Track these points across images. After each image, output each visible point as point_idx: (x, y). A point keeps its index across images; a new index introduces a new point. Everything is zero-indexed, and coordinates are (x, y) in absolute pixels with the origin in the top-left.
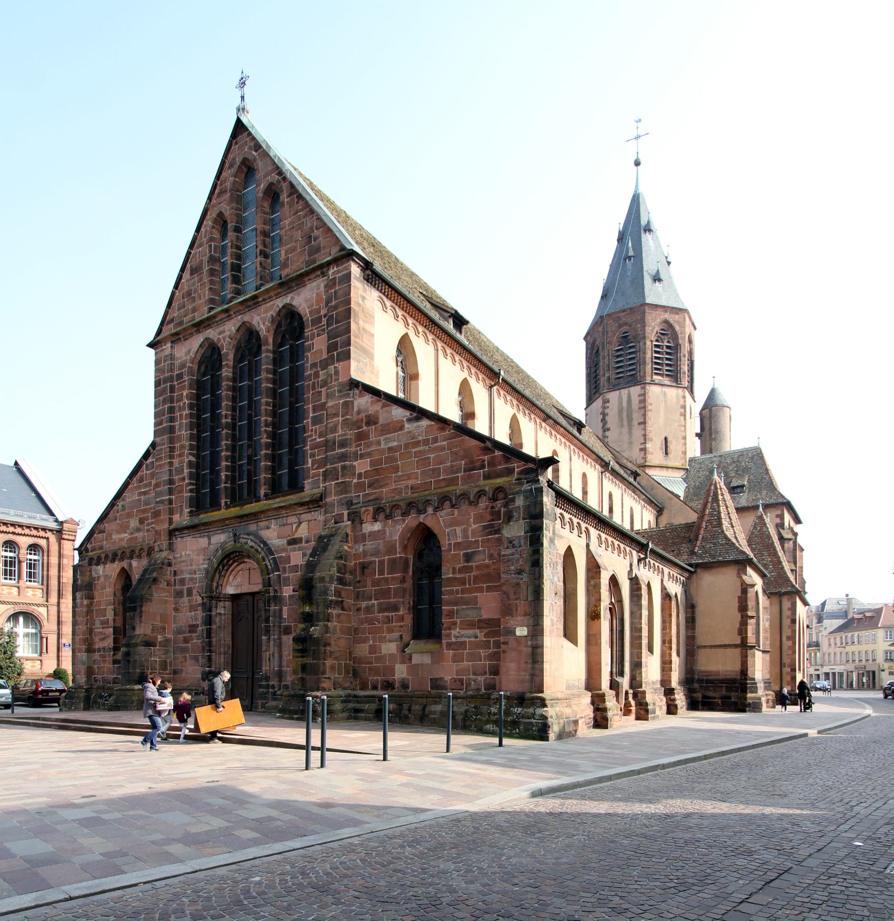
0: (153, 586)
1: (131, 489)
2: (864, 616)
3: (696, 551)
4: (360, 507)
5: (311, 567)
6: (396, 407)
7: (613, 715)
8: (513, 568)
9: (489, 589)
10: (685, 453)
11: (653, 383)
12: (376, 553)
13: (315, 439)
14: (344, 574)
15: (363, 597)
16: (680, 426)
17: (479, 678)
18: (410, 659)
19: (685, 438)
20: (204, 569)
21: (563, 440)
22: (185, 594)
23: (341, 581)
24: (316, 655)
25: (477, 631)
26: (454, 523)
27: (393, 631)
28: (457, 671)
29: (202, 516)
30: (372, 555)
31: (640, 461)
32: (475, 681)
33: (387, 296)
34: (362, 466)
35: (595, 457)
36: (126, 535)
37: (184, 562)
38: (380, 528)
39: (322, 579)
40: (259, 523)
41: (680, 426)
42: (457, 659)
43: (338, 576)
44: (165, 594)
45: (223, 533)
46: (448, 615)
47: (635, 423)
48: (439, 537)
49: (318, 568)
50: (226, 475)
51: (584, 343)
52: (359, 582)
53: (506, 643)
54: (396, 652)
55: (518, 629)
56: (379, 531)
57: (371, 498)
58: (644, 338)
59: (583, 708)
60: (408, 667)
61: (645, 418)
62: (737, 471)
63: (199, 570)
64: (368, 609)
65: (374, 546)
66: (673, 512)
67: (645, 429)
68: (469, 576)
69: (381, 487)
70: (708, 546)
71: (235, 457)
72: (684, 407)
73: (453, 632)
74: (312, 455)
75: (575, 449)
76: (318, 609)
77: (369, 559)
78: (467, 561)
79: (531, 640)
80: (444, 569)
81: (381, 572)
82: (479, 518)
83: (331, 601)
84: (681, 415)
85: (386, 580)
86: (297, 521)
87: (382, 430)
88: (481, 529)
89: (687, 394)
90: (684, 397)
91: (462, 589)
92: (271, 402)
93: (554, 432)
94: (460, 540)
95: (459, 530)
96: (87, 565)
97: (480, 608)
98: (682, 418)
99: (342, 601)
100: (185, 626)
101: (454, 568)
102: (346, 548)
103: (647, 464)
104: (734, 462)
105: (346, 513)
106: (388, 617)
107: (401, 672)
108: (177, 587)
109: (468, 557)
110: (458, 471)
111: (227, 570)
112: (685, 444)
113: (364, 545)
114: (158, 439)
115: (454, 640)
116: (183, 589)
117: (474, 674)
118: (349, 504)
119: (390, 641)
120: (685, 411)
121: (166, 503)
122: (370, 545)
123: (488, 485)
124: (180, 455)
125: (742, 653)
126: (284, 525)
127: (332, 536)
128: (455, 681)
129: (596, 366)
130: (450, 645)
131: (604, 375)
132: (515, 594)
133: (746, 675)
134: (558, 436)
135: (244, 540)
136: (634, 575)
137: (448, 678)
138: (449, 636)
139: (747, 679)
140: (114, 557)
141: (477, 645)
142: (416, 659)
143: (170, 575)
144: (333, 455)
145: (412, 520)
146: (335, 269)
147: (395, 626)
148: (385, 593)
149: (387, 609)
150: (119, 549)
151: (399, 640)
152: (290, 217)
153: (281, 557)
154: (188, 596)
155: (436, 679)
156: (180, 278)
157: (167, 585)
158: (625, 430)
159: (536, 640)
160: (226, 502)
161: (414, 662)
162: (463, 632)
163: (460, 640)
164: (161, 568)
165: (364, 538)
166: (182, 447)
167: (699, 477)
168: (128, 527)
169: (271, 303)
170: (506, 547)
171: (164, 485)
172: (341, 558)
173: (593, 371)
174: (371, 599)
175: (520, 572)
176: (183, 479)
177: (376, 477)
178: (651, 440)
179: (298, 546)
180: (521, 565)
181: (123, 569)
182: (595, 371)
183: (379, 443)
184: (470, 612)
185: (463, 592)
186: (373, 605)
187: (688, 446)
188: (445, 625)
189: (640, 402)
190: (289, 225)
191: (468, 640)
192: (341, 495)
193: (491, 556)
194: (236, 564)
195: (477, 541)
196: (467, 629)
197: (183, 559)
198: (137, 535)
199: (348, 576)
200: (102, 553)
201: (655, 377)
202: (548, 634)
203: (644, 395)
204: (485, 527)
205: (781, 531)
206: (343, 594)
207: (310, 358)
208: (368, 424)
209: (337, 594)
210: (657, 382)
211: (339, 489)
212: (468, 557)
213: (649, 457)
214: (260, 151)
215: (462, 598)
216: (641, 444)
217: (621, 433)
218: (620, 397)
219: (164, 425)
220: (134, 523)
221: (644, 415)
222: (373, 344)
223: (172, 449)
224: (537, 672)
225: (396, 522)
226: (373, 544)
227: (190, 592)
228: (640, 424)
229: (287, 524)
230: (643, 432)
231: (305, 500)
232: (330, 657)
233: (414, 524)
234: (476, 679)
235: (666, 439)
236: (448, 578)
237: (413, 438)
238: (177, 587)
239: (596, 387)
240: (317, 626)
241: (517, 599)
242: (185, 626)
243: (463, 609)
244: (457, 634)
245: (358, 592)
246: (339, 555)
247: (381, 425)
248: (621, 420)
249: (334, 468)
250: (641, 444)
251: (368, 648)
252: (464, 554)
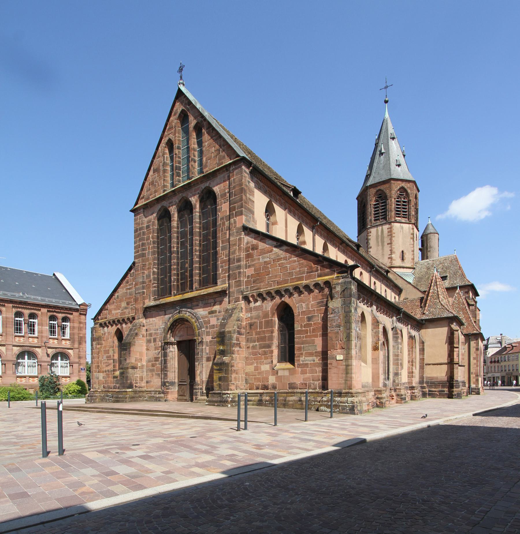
0: (136, 338)
1: (122, 287)
2: (512, 346)
3: (425, 312)
4: (249, 293)
5: (223, 325)
6: (269, 240)
7: (386, 401)
8: (334, 324)
10: (413, 259)
11: (396, 222)
12: (258, 317)
13: (223, 258)
14: (241, 329)
15: (251, 341)
16: (411, 244)
17: (316, 382)
18: (277, 373)
19: (413, 251)
20: (163, 328)
21: (350, 254)
22: (152, 341)
23: (239, 333)
24: (227, 372)
25: (314, 358)
27: (267, 359)
28: (303, 379)
29: (161, 300)
30: (255, 319)
31: (389, 265)
32: (313, 384)
33: (261, 181)
34: (250, 272)
35: (366, 263)
36: (120, 311)
37: (151, 324)
38: (260, 304)
39: (230, 332)
40: (192, 303)
41: (411, 244)
42: (304, 372)
43: (237, 330)
44: (142, 341)
45: (173, 308)
46: (298, 350)
47: (386, 244)
48: (293, 308)
49: (227, 326)
50: (174, 278)
51: (356, 202)
52: (248, 333)
53: (331, 364)
54: (269, 369)
55: (337, 356)
56: (259, 306)
57: (255, 288)
58: (391, 197)
59: (371, 397)
60: (276, 378)
61: (391, 241)
62: (443, 268)
63: (160, 328)
64: (254, 347)
65: (256, 314)
66: (408, 291)
67: (391, 247)
68: (310, 329)
69: (260, 282)
70: (431, 310)
71: (179, 268)
72: (413, 234)
73: (301, 359)
74: (222, 267)
75: (357, 259)
76: (227, 348)
77: (254, 321)
78: (309, 320)
79: (345, 362)
80: (296, 325)
81: (261, 327)
82: (314, 299)
83: (234, 343)
84: (411, 239)
85: (264, 332)
86: (214, 301)
87: (260, 253)
88: (316, 304)
89: (414, 227)
90: (413, 229)
91: (306, 336)
92: (198, 239)
93: (346, 251)
94: (304, 310)
96: (98, 327)
97: (316, 346)
98: (412, 240)
99: (240, 343)
100: (152, 358)
101: (301, 325)
102: (241, 315)
103: (392, 266)
104: (441, 263)
105: (241, 297)
106: (265, 351)
107: (272, 380)
108: (148, 338)
109: (309, 319)
110: (304, 273)
111: (175, 328)
112: (413, 254)
113: (251, 314)
114: (136, 260)
115: (301, 362)
116: (151, 339)
117: (313, 380)
118: (242, 293)
119: (266, 364)
120: (413, 236)
121: (141, 294)
122: (254, 313)
124: (149, 268)
125: (451, 367)
126: (207, 304)
127: (234, 309)
128: (302, 384)
129: (363, 213)
130: (299, 365)
132: (336, 337)
133: (453, 379)
134: (348, 252)
135: (185, 312)
136: (394, 326)
137: (298, 383)
138: (299, 360)
139: (453, 381)
140: (113, 323)
141: (315, 365)
142: (280, 373)
143: (144, 331)
144: (233, 266)
145: (278, 300)
146: (234, 167)
147: (269, 356)
148: (263, 339)
149: (264, 347)
150: (116, 319)
151: (271, 363)
152: (208, 141)
153: (205, 321)
154: (154, 342)
155: (292, 384)
156: (147, 174)
157: (143, 337)
158: (380, 247)
159: (348, 362)
160: (174, 292)
161: (279, 375)
162: (306, 358)
163: (305, 362)
164: (139, 328)
166: (150, 264)
167: (421, 272)
168: (120, 307)
169: (198, 186)
170: (331, 313)
171: (140, 284)
172: (239, 320)
173: (361, 216)
174: (255, 342)
176: (151, 281)
177: (257, 278)
178: (394, 253)
179: (214, 315)
180: (339, 323)
181: (118, 329)
182: (363, 216)
183: (259, 259)
184: (310, 348)
186: (256, 345)
187: (415, 255)
188: (296, 355)
189: (388, 232)
190: (208, 145)
191: (309, 362)
192: (238, 287)
194: (180, 325)
195: (314, 310)
196: (309, 357)
197: (151, 323)
198: (125, 311)
199: (243, 331)
200: (107, 320)
201: (397, 218)
202: (354, 358)
203: (391, 228)
204: (318, 303)
205: (468, 300)
206: (240, 339)
207: (220, 215)
208: (253, 249)
209: (237, 339)
210: (398, 221)
211: (237, 284)
212: (309, 319)
213: (394, 262)
214: (191, 105)
215: (306, 340)
216: (389, 255)
217: (377, 250)
218: (377, 231)
219: (140, 253)
220: (124, 304)
221: (391, 239)
222: (254, 206)
223: (144, 265)
224: (349, 379)
225: (269, 301)
226: (256, 313)
227: (155, 340)
228: (388, 244)
229: (208, 303)
230: (390, 249)
231: (218, 290)
232: (234, 373)
233: (280, 301)
234: (314, 383)
235: (403, 252)
236: (298, 330)
237: (278, 256)
238: (148, 338)
239: (363, 225)
240: (227, 356)
241: (337, 340)
242: (153, 358)
243: (307, 346)
244: (303, 360)
245: (248, 338)
246: (238, 319)
247: (260, 250)
248: (378, 242)
249: (234, 273)
250: (389, 255)
251: (253, 367)
252: (307, 317)
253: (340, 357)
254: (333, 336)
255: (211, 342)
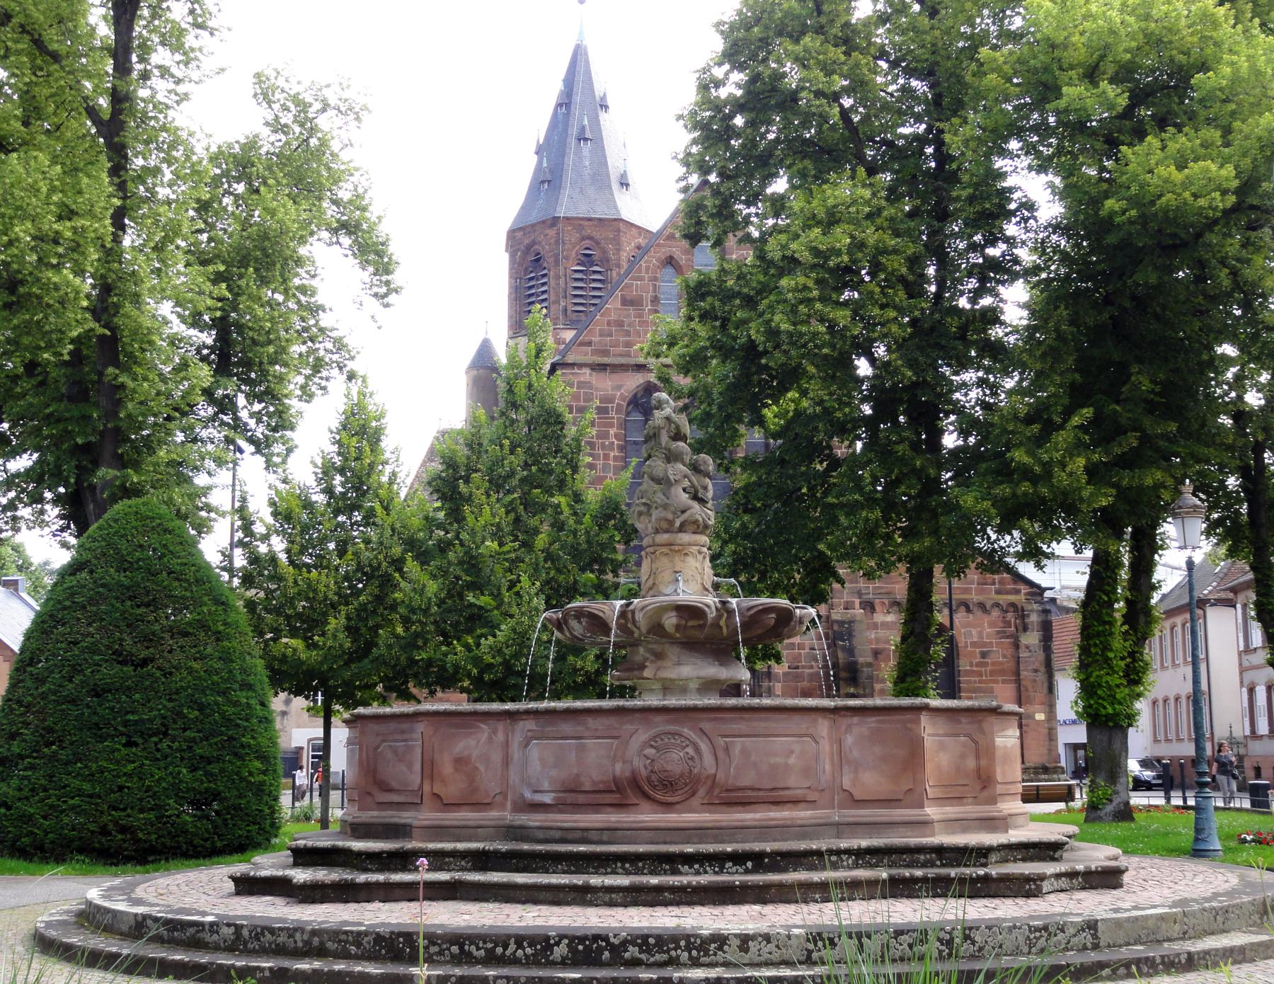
9: (1004, 682)
26: (969, 625)
77: (881, 646)
82: (992, 625)
95: (974, 632)
105: (857, 601)
109: (984, 655)
118: (859, 594)
123: (1005, 599)
131: (557, 302)
165: (875, 626)
175: (1036, 671)
185: (980, 682)
193: (1004, 656)
204: (999, 632)
212: (984, 655)
253: (1040, 717)
254: (1030, 686)
255: (785, 674)
